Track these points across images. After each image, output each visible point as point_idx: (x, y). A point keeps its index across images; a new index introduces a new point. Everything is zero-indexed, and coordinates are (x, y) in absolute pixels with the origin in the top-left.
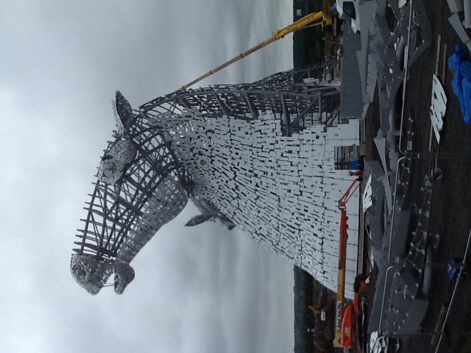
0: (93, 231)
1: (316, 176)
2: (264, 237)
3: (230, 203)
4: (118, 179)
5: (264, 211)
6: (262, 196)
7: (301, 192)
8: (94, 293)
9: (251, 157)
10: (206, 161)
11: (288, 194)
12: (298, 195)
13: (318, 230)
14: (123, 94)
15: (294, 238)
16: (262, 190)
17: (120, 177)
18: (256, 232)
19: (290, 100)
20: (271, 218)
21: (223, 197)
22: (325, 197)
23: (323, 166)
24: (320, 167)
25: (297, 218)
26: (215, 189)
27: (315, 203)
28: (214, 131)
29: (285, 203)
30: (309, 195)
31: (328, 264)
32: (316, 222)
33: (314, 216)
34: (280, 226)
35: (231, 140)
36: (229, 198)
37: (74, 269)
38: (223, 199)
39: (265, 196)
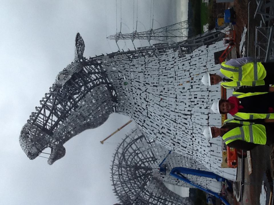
0: (43, 113)
3: (141, 113)
5: (165, 109)
6: (164, 98)
7: (192, 86)
8: (32, 159)
9: (158, 75)
13: (205, 108)
14: (81, 35)
15: (186, 124)
16: (166, 94)
18: (159, 133)
19: (185, 53)
23: (206, 66)
24: (205, 66)
25: (189, 106)
26: (132, 105)
27: (202, 90)
29: (180, 98)
30: (198, 86)
32: (203, 103)
33: (201, 99)
34: (177, 117)
35: (145, 68)
36: (141, 110)
37: (22, 132)
38: (137, 112)
39: (166, 97)
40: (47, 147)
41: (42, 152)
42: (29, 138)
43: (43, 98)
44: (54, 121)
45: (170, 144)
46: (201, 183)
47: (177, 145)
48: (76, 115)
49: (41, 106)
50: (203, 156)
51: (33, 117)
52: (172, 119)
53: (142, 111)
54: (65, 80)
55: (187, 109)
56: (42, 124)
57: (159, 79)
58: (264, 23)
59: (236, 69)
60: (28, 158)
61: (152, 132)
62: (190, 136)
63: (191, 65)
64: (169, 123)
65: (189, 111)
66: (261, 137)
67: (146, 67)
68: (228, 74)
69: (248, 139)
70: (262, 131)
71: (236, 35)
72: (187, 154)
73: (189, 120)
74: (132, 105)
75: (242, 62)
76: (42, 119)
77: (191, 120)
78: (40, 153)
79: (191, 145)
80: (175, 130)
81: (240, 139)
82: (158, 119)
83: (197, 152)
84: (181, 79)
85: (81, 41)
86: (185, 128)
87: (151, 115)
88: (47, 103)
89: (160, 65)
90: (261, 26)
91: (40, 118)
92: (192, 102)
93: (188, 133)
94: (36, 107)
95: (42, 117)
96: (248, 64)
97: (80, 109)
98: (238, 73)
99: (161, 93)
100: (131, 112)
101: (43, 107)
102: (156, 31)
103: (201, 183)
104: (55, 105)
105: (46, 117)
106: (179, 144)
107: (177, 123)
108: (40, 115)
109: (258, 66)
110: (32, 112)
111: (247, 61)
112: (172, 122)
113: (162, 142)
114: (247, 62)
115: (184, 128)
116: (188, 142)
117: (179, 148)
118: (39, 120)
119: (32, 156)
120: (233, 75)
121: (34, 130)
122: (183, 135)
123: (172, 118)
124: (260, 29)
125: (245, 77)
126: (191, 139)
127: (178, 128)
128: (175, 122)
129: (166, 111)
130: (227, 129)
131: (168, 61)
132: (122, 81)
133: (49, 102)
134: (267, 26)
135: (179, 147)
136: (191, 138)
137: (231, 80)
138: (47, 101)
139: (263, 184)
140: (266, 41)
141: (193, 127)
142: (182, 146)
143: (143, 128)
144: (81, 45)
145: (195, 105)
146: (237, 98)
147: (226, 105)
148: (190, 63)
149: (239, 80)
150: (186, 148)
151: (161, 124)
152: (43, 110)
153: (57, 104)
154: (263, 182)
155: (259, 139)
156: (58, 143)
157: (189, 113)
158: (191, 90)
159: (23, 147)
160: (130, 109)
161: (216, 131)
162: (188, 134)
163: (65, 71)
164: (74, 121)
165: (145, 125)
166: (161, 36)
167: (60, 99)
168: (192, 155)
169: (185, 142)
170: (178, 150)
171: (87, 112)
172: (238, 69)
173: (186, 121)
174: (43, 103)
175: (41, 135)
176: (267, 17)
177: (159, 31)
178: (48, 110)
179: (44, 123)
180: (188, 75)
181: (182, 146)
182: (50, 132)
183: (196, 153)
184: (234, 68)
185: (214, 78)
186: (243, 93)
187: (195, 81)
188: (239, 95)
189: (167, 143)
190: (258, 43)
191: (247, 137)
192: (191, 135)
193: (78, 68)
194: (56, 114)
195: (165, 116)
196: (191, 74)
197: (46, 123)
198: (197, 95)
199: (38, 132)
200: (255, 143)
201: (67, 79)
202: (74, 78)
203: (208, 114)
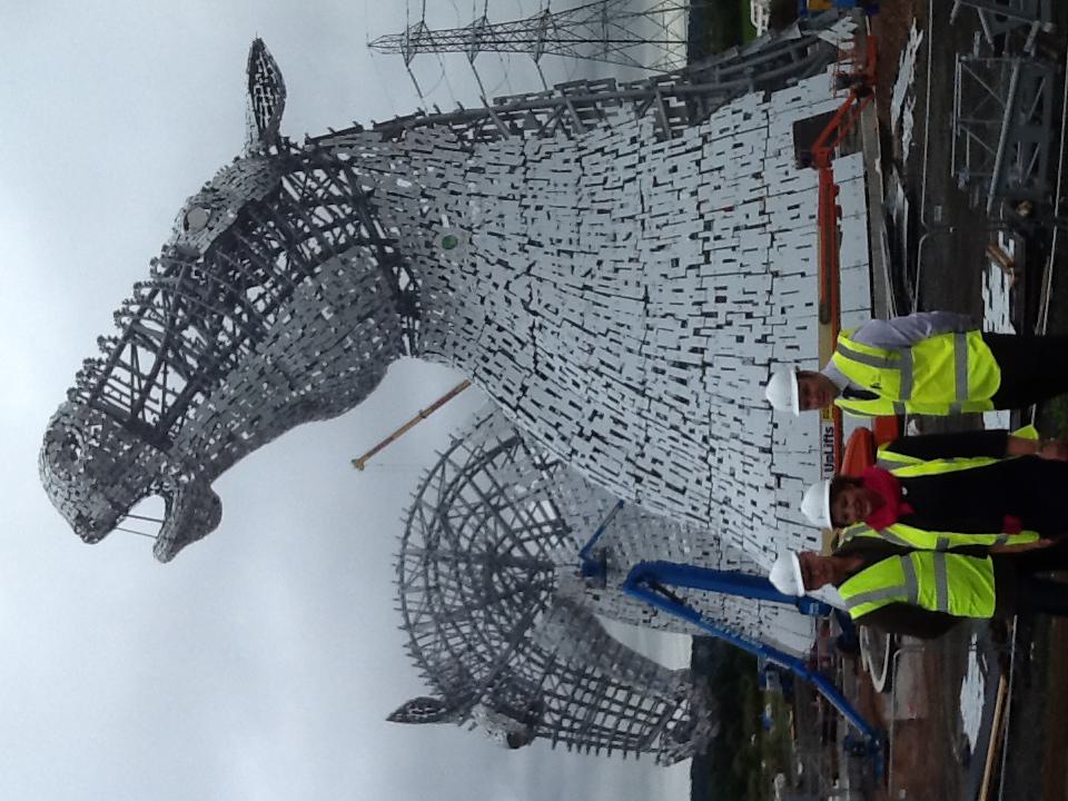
0: (128, 362)
1: (745, 202)
2: (602, 439)
3: (511, 358)
4: (221, 231)
5: (604, 342)
6: (601, 300)
7: (707, 254)
8: (90, 540)
10: (459, 237)
11: (672, 272)
12: (698, 266)
13: (758, 341)
14: (270, 48)
15: (685, 401)
16: (605, 282)
17: (226, 228)
18: (581, 434)
19: (678, 120)
20: (626, 356)
21: (495, 348)
22: (772, 246)
23: (763, 174)
24: (757, 176)
25: (697, 332)
26: (476, 328)
27: (744, 270)
28: (484, 169)
29: (662, 299)
30: (729, 254)
31: (790, 447)
32: (750, 321)
33: (743, 305)
34: (651, 376)
35: (526, 181)
36: (510, 344)
37: (50, 438)
38: (495, 353)
39: (609, 296)
40: (148, 494)
41: (131, 513)
42: (77, 462)
43: (127, 303)
44: (173, 393)
45: (624, 477)
46: (737, 618)
47: (650, 482)
48: (258, 369)
49: (120, 334)
50: (747, 522)
51: (89, 378)
52: (629, 382)
53: (515, 351)
54: (211, 229)
55: (686, 345)
56: (126, 405)
57: (579, 224)
58: (990, 41)
59: (890, 358)
60: (78, 538)
61: (553, 432)
62: (700, 446)
63: (703, 169)
64: (618, 397)
65: (694, 350)
66: (978, 594)
67: (528, 177)
68: (863, 376)
69: (931, 602)
70: (977, 572)
71: (878, 59)
73: (695, 385)
74: (476, 328)
75: (913, 333)
76: (127, 385)
77: (705, 388)
78: (121, 517)
79: (705, 483)
80: (644, 426)
81: (905, 599)
82: (578, 380)
83: (724, 507)
84: (666, 225)
85: (269, 71)
86: (681, 416)
87: (548, 365)
88: (143, 322)
89: (583, 168)
90: (976, 50)
91: (118, 380)
92: (704, 314)
93: (692, 436)
94: (101, 340)
95: (126, 376)
96: (936, 341)
98: (899, 371)
99: (588, 281)
100: (470, 355)
101: (126, 338)
102: (564, 19)
104: (173, 330)
105: (141, 377)
106: (658, 476)
107: (650, 399)
108: (117, 371)
109: (970, 348)
110: (86, 357)
111: (929, 329)
112: (631, 394)
113: (591, 470)
114: (931, 332)
115: (675, 418)
116: (691, 471)
117: (659, 491)
118: (114, 389)
119: (93, 528)
120: (880, 379)
121: (96, 430)
122: (673, 443)
123: (629, 379)
124: (978, 66)
125: (924, 387)
126: (705, 460)
127: (652, 416)
128: (644, 395)
129: (608, 350)
130: (855, 563)
131: (614, 155)
132: (437, 233)
133: (149, 318)
134: (998, 53)
136: (704, 454)
137: (875, 397)
138: (141, 313)
139: (974, 647)
140: (993, 109)
141: (710, 413)
142: (668, 485)
143: (518, 417)
144: (268, 89)
145: (719, 327)
146: (891, 475)
147: (854, 504)
148: (698, 163)
149: (900, 398)
150: (683, 492)
151: (589, 402)
152: (128, 348)
153: (184, 327)
154: (974, 640)
155: (969, 602)
156: (193, 477)
157: (696, 359)
158: (705, 270)
159: (56, 493)
160: (468, 340)
161: (817, 573)
162: (692, 440)
163: (210, 196)
164: (251, 391)
165: (525, 403)
166: (585, 41)
167: (193, 303)
168: (707, 518)
169: (679, 469)
170: (658, 503)
171: (301, 354)
172: (898, 357)
173: (684, 392)
174: (128, 323)
175: (126, 447)
176: (1001, 19)
177: (577, 17)
178: (148, 349)
179: (133, 401)
180: (692, 211)
181: (668, 485)
182: (159, 436)
183: (723, 512)
184: (883, 356)
185: (813, 388)
186: (920, 461)
187: (717, 234)
188: (900, 465)
189: (614, 474)
190: (964, 120)
191: (925, 592)
192: (705, 445)
193: (263, 181)
194: (181, 366)
195: (603, 369)
196: (704, 208)
197: (142, 400)
198: (725, 288)
199: (110, 436)
200: (955, 613)
201: (219, 228)
202: (245, 220)
203: (766, 362)
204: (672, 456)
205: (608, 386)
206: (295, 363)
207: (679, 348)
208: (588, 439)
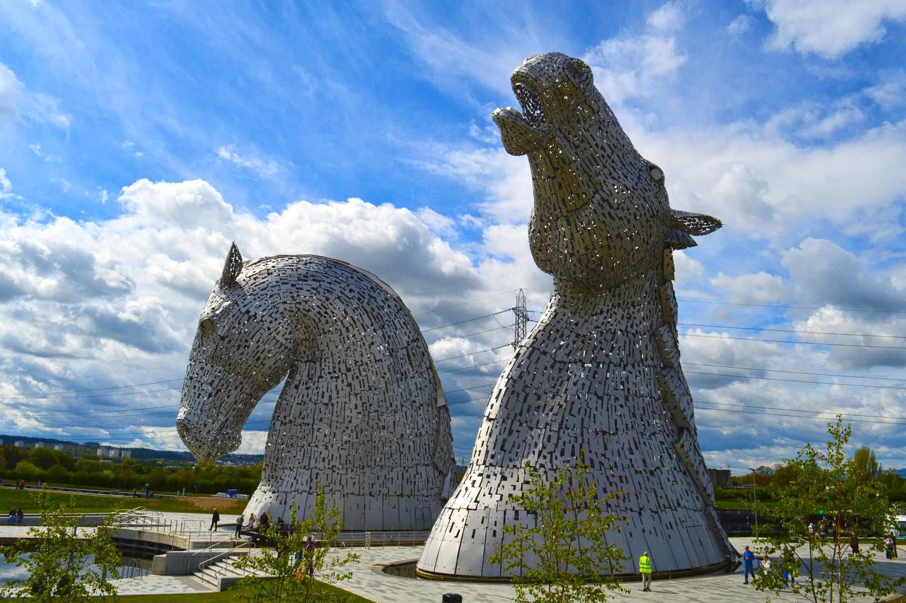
14: (718, 231)
15: (562, 454)
39: (608, 410)
55: (593, 456)
65: (592, 461)
72: (487, 452)
83: (499, 477)
85: (704, 229)
93: (541, 457)
97: (599, 204)
103: (278, 479)
117: (500, 434)
123: (567, 420)
135: (502, 432)
157: (588, 463)
165: (537, 354)
168: (487, 464)
181: (505, 440)
183: (495, 475)
198: (627, 482)
204: (523, 444)
205: (561, 406)
206: (586, 215)
207: (590, 452)
208: (523, 391)
